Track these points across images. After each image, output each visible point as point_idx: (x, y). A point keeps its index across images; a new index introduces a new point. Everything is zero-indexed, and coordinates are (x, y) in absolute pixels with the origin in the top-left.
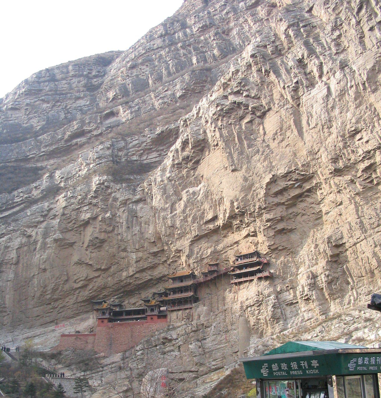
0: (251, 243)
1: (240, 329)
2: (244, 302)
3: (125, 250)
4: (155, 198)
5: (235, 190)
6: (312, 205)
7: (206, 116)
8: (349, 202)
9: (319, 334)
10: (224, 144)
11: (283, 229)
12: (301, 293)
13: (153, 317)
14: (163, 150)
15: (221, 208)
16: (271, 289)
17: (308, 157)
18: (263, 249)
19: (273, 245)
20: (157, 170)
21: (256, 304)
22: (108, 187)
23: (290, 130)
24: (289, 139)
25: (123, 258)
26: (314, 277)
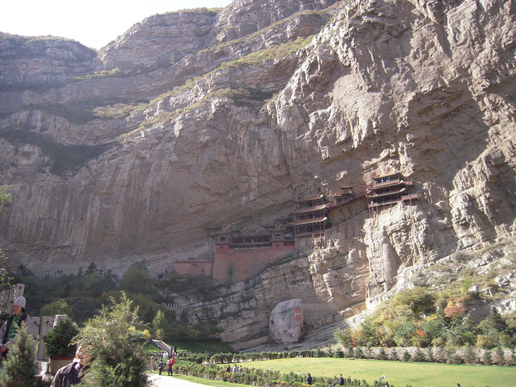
0: (391, 165)
1: (385, 256)
2: (387, 227)
3: (246, 174)
4: (280, 121)
5: (372, 109)
6: (460, 125)
7: (337, 37)
8: (508, 119)
9: (487, 262)
10: (358, 64)
11: (429, 150)
12: (457, 217)
13: (278, 243)
14: (280, 80)
15: (356, 129)
16: (421, 213)
17: (456, 74)
18: (407, 172)
20: (281, 94)
22: (228, 110)
23: (433, 48)
24: (433, 56)
25: (244, 182)
26: (471, 200)
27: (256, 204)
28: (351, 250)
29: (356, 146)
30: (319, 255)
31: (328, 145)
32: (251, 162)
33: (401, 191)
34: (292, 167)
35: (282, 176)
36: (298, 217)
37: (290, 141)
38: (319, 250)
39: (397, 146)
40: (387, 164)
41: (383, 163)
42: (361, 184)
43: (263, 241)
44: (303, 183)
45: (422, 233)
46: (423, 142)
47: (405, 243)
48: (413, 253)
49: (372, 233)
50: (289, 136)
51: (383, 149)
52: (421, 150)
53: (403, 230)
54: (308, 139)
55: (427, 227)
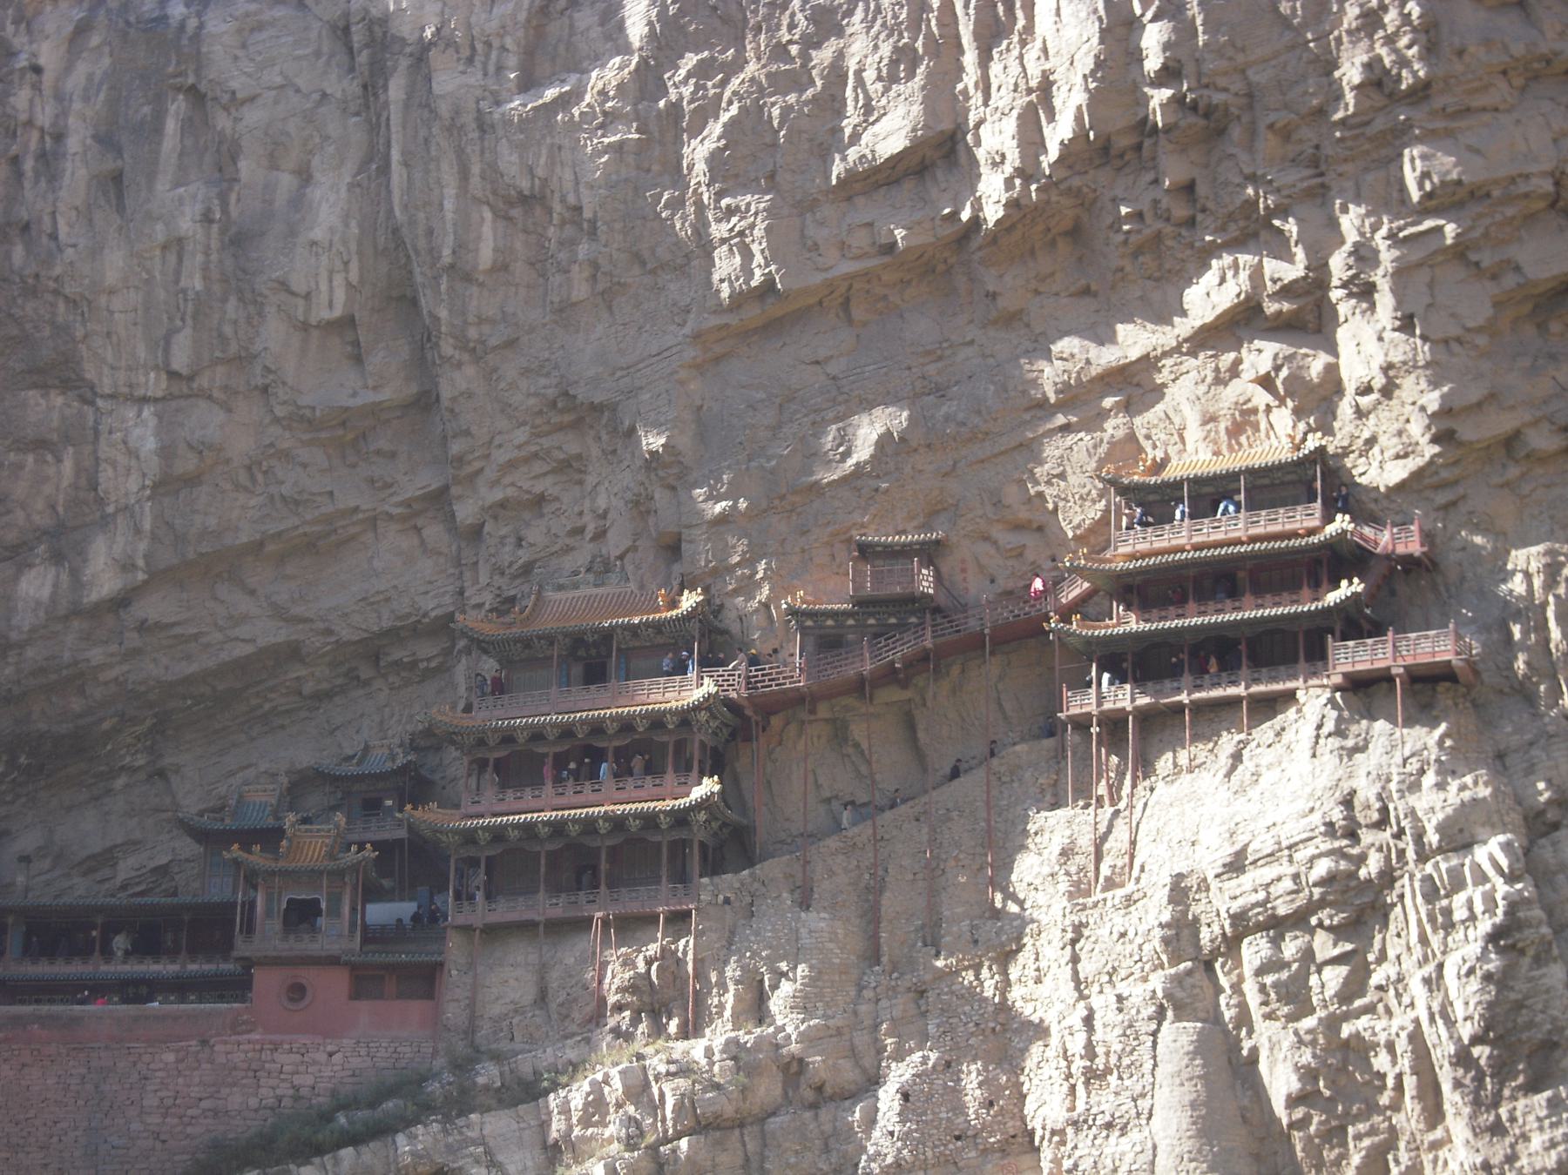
0: (1266, 382)
2: (1204, 886)
13: (307, 975)
15: (1003, 71)
16: (1476, 786)
19: (1479, 405)
21: (1322, 904)
25: (41, 445)
27: (133, 639)
28: (899, 1056)
29: (993, 213)
30: (638, 1090)
31: (772, 182)
32: (111, 278)
33: (1332, 598)
34: (463, 343)
35: (374, 410)
36: (482, 765)
37: (454, 128)
38: (638, 1045)
39: (1323, 238)
40: (1234, 371)
41: (1199, 366)
42: (1019, 527)
43: (173, 954)
44: (538, 488)
45: (1474, 949)
46: (1530, 218)
47: (1332, 1024)
48: (1396, 1106)
49: (1078, 929)
50: (448, 80)
51: (1212, 251)
52: (1510, 281)
53: (1324, 915)
54: (610, 120)
55: (1513, 906)
